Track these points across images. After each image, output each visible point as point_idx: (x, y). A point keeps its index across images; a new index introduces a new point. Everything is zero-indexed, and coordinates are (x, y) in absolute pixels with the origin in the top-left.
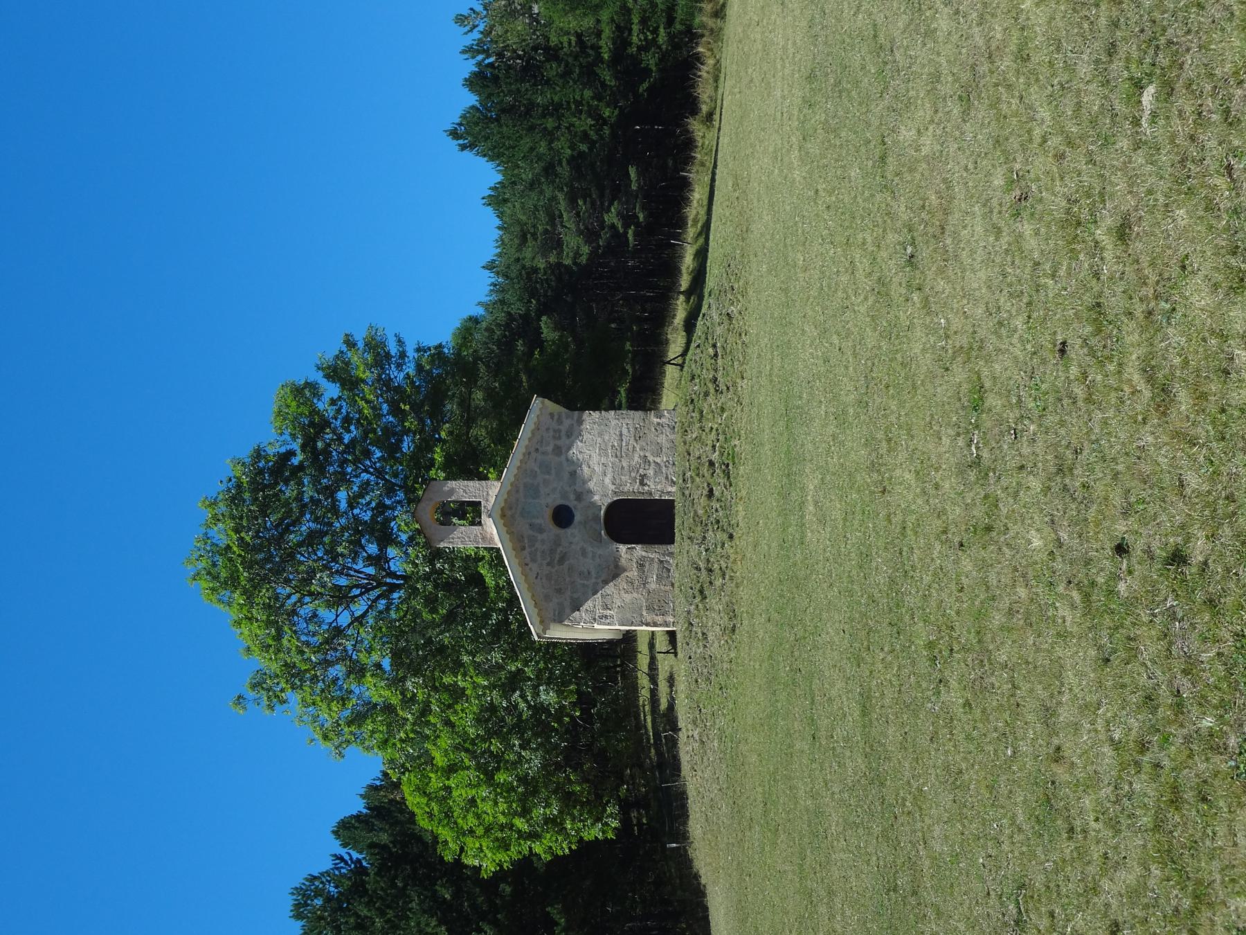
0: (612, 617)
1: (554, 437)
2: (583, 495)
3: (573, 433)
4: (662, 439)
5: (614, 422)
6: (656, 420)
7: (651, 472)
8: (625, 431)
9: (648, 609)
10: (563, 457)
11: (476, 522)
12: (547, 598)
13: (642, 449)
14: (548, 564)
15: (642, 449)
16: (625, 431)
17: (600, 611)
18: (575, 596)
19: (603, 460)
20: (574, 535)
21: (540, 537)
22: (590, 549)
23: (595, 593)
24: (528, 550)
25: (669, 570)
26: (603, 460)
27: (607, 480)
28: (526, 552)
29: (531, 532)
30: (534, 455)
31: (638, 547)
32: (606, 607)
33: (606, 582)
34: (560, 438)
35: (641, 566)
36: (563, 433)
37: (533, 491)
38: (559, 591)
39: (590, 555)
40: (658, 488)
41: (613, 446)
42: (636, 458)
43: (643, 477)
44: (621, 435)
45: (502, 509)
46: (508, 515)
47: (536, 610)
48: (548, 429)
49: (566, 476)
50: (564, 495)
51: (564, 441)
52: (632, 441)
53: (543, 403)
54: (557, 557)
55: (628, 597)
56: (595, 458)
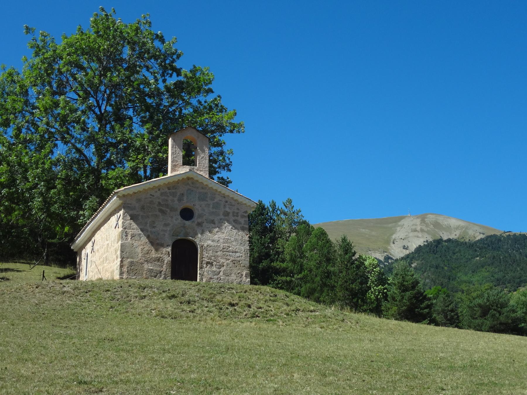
0: (127, 239)
1: (234, 212)
2: (202, 228)
3: (236, 224)
4: (233, 277)
5: (243, 248)
6: (244, 273)
7: (214, 269)
8: (238, 254)
9: (132, 263)
10: (222, 217)
11: (185, 163)
12: (139, 200)
13: (228, 264)
14: (159, 203)
15: (228, 264)
16: (238, 254)
17: (130, 232)
18: (140, 217)
19: (221, 240)
20: (177, 220)
21: (176, 199)
22: (168, 229)
23: (142, 230)
24: (168, 191)
25: (155, 277)
26: (221, 240)
27: (210, 242)
28: (167, 190)
29: (178, 194)
30: (224, 200)
31: (170, 259)
32: (133, 236)
33: (148, 237)
34: (234, 216)
35: (158, 260)
36: (236, 218)
37: (203, 198)
38: (143, 208)
39: (165, 229)
40: (204, 273)
41: (229, 247)
42: (222, 261)
43: (212, 264)
44: (236, 252)
45: (192, 178)
46: (187, 181)
47: (131, 193)
48: (238, 209)
49: (211, 218)
50: (200, 216)
51: (232, 218)
52: (232, 259)
53: (253, 207)
54: (164, 209)
55: (139, 250)
56: (223, 236)
